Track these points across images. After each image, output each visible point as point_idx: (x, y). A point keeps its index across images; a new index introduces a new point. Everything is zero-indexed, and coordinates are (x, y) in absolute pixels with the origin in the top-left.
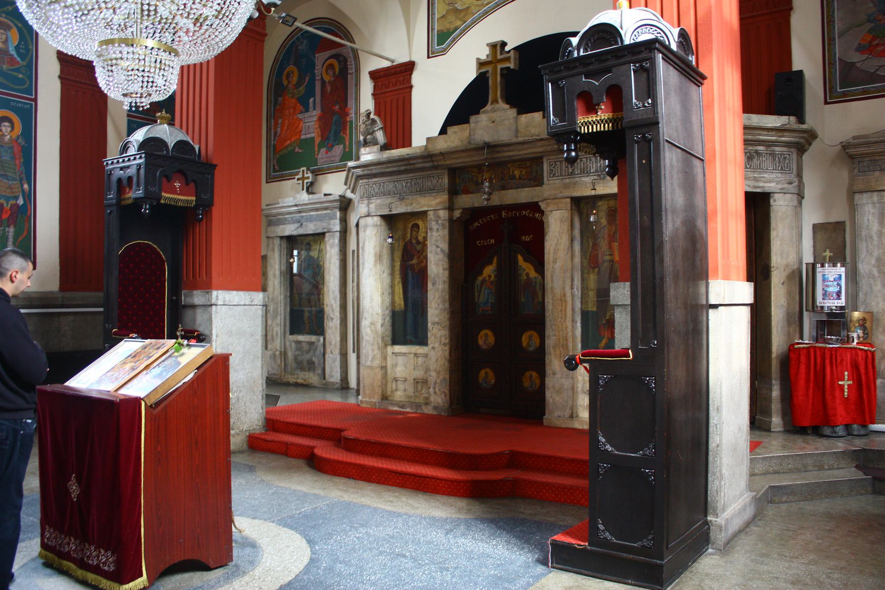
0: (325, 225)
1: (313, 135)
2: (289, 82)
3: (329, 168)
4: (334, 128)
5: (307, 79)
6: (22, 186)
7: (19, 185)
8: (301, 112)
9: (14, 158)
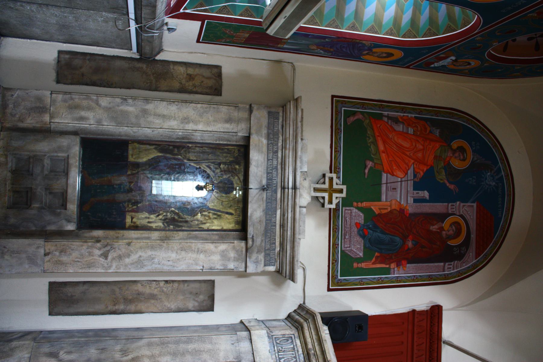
0: (258, 241)
1: (384, 197)
2: (454, 151)
3: (336, 230)
4: (386, 238)
5: (452, 187)
8: (415, 176)
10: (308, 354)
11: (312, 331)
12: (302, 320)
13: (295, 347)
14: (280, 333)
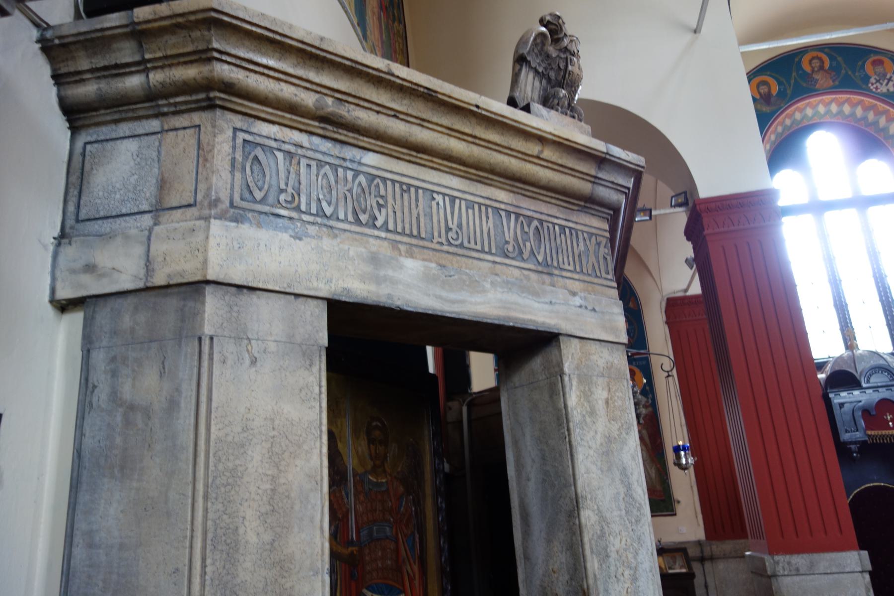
10: (326, 119)
11: (264, 61)
12: (190, 73)
13: (287, 147)
14: (226, 175)
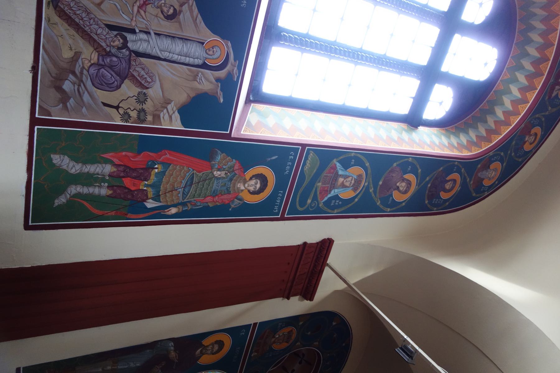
6: (175, 206)
7: (176, 202)
9: (214, 194)
